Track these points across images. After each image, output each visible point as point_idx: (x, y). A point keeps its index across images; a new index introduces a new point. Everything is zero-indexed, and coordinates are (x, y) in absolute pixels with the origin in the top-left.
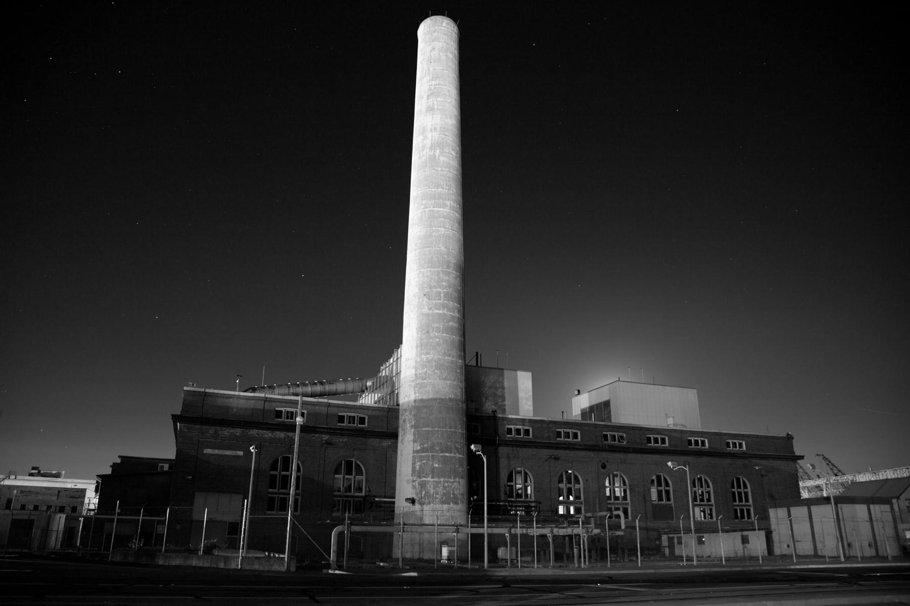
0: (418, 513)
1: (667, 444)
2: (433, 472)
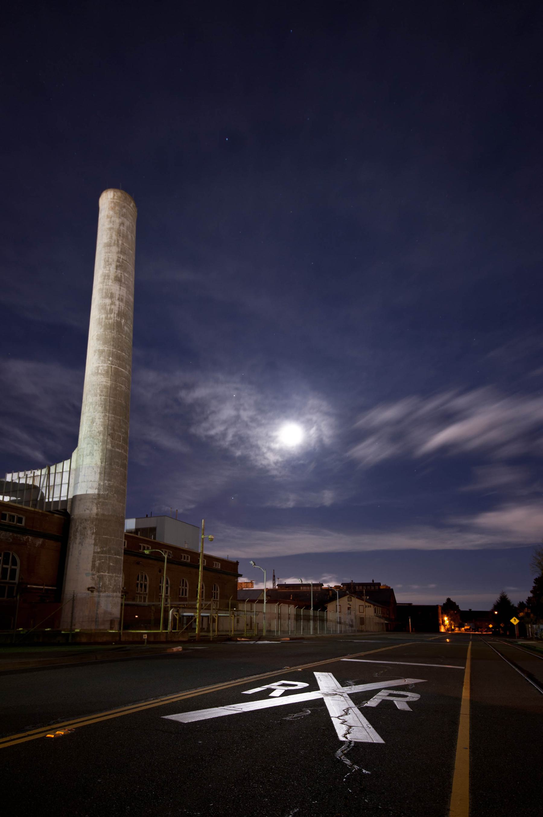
0: (96, 599)
1: (189, 561)
2: (110, 569)
